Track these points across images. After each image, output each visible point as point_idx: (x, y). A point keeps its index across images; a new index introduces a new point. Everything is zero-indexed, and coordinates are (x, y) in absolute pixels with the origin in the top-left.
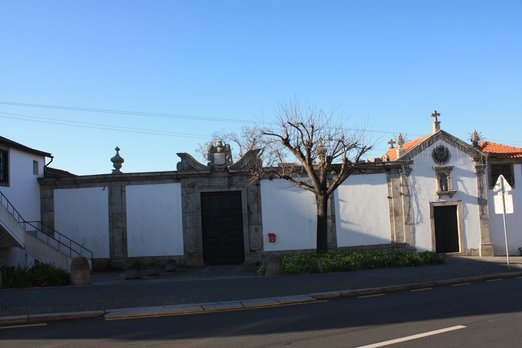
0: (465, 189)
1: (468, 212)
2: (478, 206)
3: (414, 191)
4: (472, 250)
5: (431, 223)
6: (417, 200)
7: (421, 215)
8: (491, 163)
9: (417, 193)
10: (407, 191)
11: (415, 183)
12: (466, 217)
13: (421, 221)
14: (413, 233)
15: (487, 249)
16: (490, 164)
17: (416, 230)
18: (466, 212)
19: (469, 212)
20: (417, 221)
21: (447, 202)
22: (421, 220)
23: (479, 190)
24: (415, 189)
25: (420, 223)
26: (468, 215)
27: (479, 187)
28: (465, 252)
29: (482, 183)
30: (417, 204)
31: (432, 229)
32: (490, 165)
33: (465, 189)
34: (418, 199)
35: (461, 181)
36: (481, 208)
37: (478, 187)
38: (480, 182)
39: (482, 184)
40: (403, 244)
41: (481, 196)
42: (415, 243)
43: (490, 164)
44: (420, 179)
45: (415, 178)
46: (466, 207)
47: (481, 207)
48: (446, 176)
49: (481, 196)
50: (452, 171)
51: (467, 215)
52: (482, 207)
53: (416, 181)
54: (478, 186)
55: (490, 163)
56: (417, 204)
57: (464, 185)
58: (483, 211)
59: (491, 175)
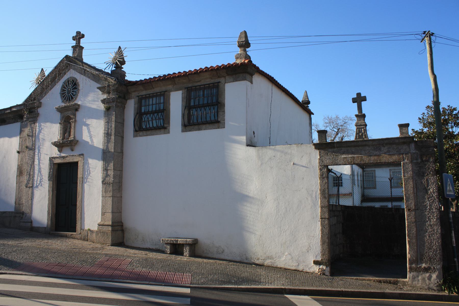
0: (91, 137)
1: (90, 173)
3: (38, 143)
4: (89, 231)
5: (49, 187)
6: (39, 154)
7: (41, 176)
8: (139, 95)
9: (40, 145)
10: (32, 143)
11: (40, 132)
12: (87, 180)
13: (40, 184)
14: (32, 199)
15: (103, 232)
16: (137, 96)
17: (34, 196)
18: (87, 171)
19: (91, 172)
20: (37, 183)
21: (67, 156)
22: (41, 182)
23: (106, 138)
24: (40, 140)
25: (39, 187)
26: (89, 177)
27: (106, 132)
28: (80, 233)
29: (111, 126)
30: (39, 160)
31: (49, 195)
32: (137, 98)
33: (91, 137)
34: (40, 153)
35: (87, 125)
36: (106, 166)
38: (108, 125)
39: (110, 128)
40: (20, 213)
41: (107, 146)
42: (31, 213)
44: (45, 125)
45: (41, 125)
46: (89, 165)
47: (106, 164)
48: (71, 119)
49: (107, 146)
50: (79, 112)
51: (88, 177)
52: (106, 165)
53: (42, 129)
56: (39, 160)
57: (89, 132)
58: (108, 170)
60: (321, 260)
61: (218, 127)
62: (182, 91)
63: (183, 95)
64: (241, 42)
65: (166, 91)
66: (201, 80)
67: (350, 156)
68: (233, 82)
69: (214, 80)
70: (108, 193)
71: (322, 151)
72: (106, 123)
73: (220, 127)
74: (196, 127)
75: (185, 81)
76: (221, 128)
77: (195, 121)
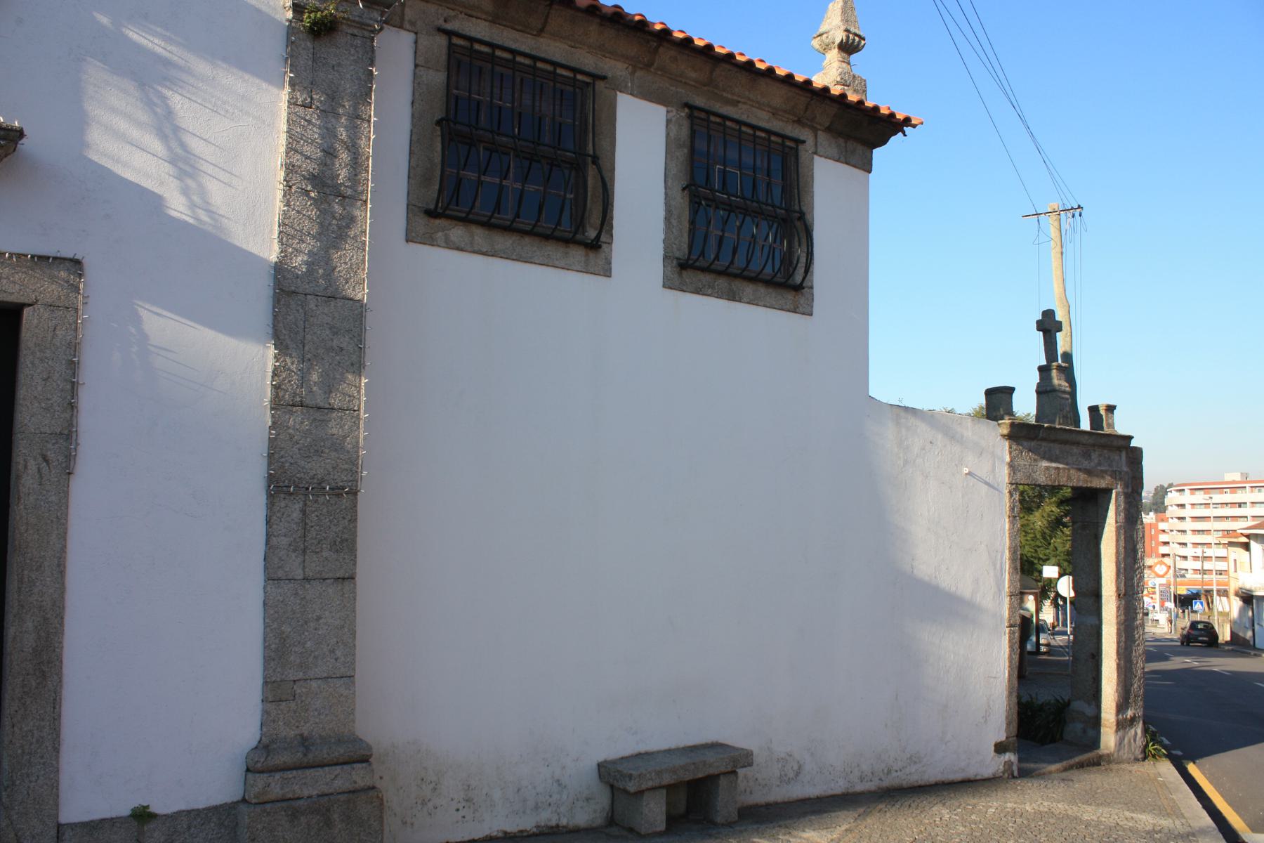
2: (271, 351)
8: (449, 26)
16: (441, 30)
27: (312, 167)
36: (303, 379)
37: (290, 169)
43: (441, 30)
49: (321, 260)
54: (297, 159)
55: (441, 22)
59: (439, 123)
60: (1007, 738)
61: (795, 309)
62: (668, 112)
63: (674, 129)
64: (856, 35)
65: (604, 78)
66: (739, 102)
67: (1054, 465)
68: (838, 161)
69: (781, 123)
70: (325, 554)
71: (1014, 447)
72: (300, 110)
73: (801, 309)
74: (722, 282)
75: (694, 75)
76: (803, 314)
77: (740, 261)
